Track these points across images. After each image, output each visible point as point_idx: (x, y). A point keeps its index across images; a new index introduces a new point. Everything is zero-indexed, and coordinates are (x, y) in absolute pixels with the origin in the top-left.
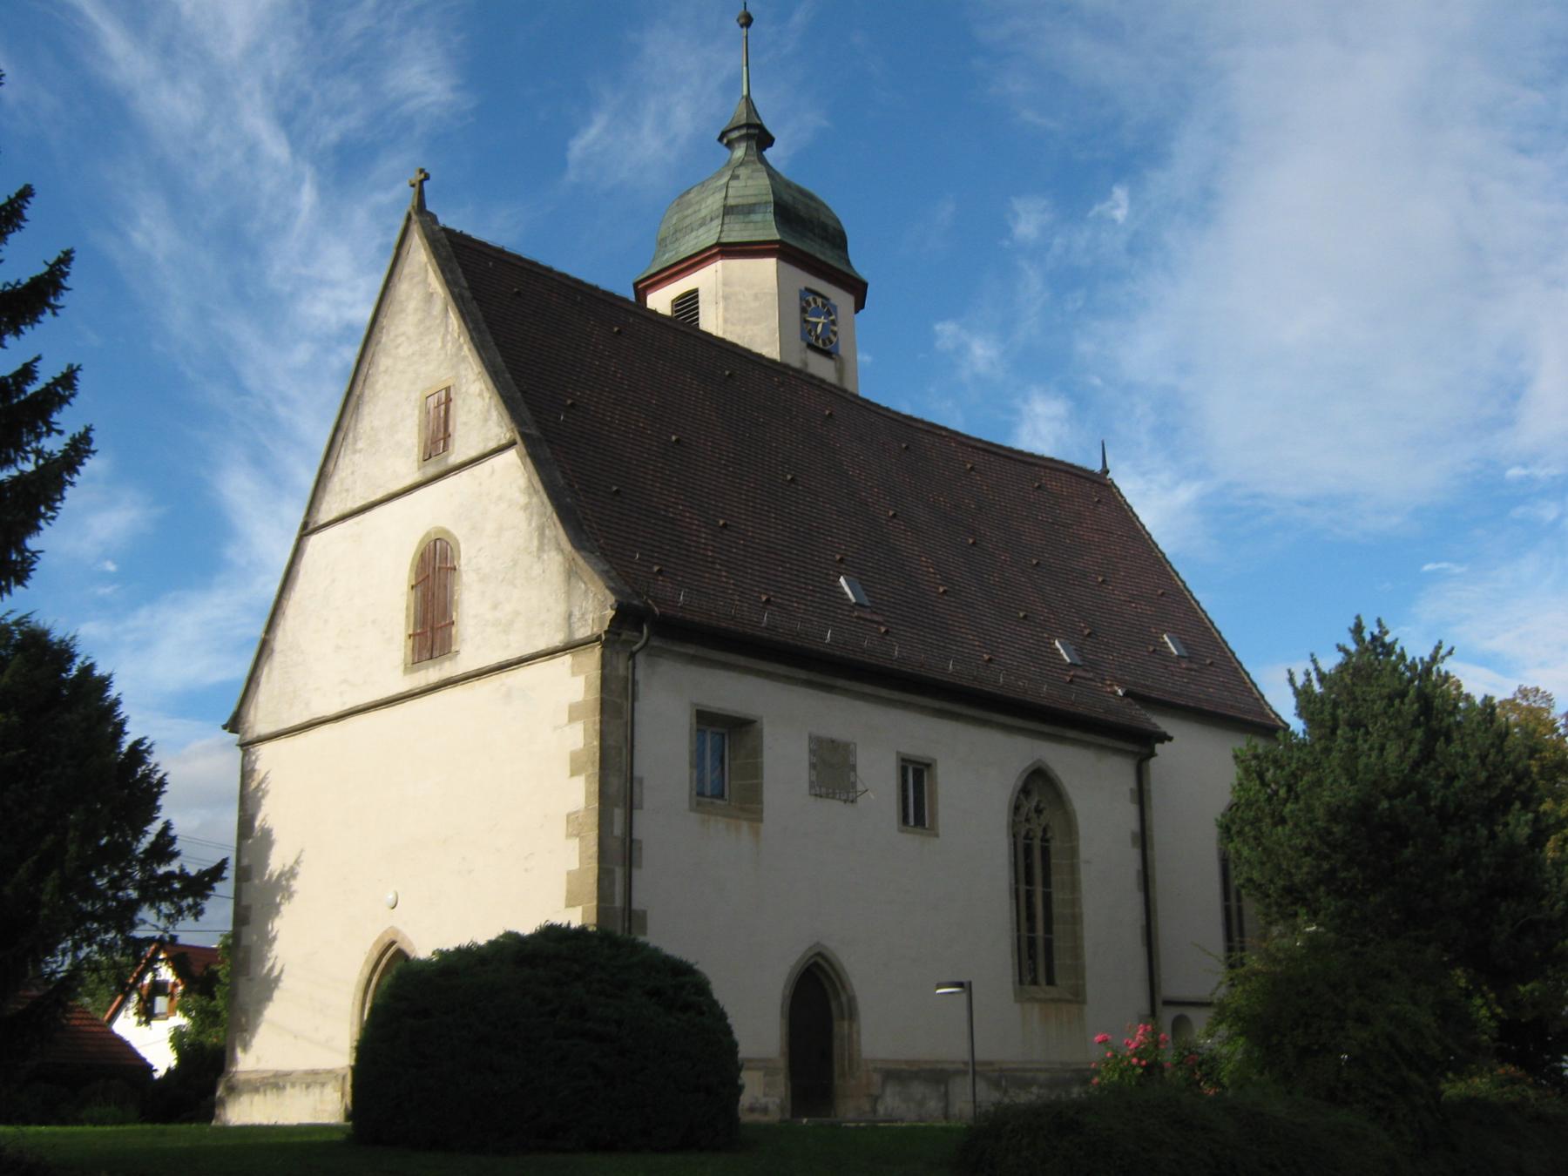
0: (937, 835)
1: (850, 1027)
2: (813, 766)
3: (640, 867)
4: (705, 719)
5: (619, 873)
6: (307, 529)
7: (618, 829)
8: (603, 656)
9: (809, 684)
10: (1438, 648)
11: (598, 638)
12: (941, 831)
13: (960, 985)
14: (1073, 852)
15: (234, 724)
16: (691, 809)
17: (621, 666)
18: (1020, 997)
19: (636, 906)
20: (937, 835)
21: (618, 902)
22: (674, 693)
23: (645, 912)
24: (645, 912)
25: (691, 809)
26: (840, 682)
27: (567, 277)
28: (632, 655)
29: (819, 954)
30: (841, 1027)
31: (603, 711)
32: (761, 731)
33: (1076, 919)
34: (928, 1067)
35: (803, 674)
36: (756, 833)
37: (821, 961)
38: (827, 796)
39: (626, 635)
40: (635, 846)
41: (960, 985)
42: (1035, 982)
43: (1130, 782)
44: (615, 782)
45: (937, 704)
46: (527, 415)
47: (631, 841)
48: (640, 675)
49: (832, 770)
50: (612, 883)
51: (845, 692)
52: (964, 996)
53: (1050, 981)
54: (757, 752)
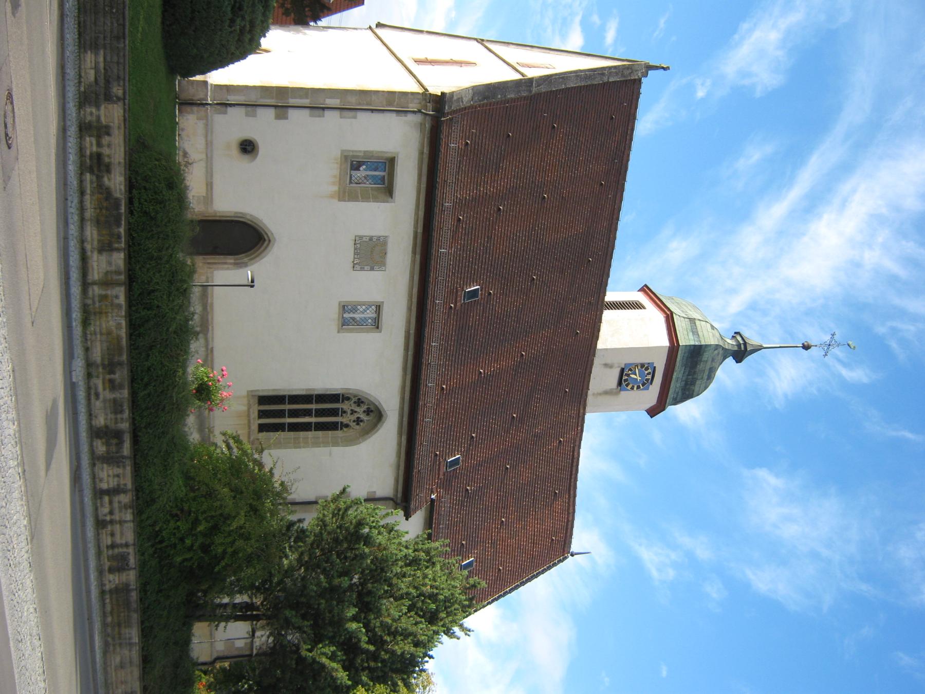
0: (338, 332)
1: (231, 264)
2: (371, 238)
3: (311, 116)
4: (390, 163)
5: (306, 102)
6: (481, 41)
7: (330, 102)
8: (418, 93)
9: (416, 234)
10: (469, 631)
11: (426, 90)
12: (340, 334)
13: (253, 281)
14: (336, 444)
15: (379, 25)
16: (343, 151)
17: (413, 107)
18: (251, 394)
19: (291, 112)
20: (338, 332)
21: (292, 101)
22: (401, 139)
23: (287, 118)
24: (287, 118)
25: (343, 151)
26: (418, 257)
27: (628, 160)
28: (419, 111)
29: (270, 241)
30: (230, 260)
31: (389, 92)
32: (387, 202)
33: (297, 445)
34: (210, 317)
35: (420, 230)
36: (332, 197)
37: (266, 243)
38: (355, 249)
39: (430, 105)
40: (321, 112)
41: (253, 281)
42: (262, 414)
43: (380, 493)
44: (352, 101)
45: (412, 332)
46: (543, 89)
47: (323, 109)
48: (410, 117)
49: (369, 253)
50: (301, 97)
51: (413, 262)
52: (246, 283)
53: (262, 428)
54: (376, 199)
